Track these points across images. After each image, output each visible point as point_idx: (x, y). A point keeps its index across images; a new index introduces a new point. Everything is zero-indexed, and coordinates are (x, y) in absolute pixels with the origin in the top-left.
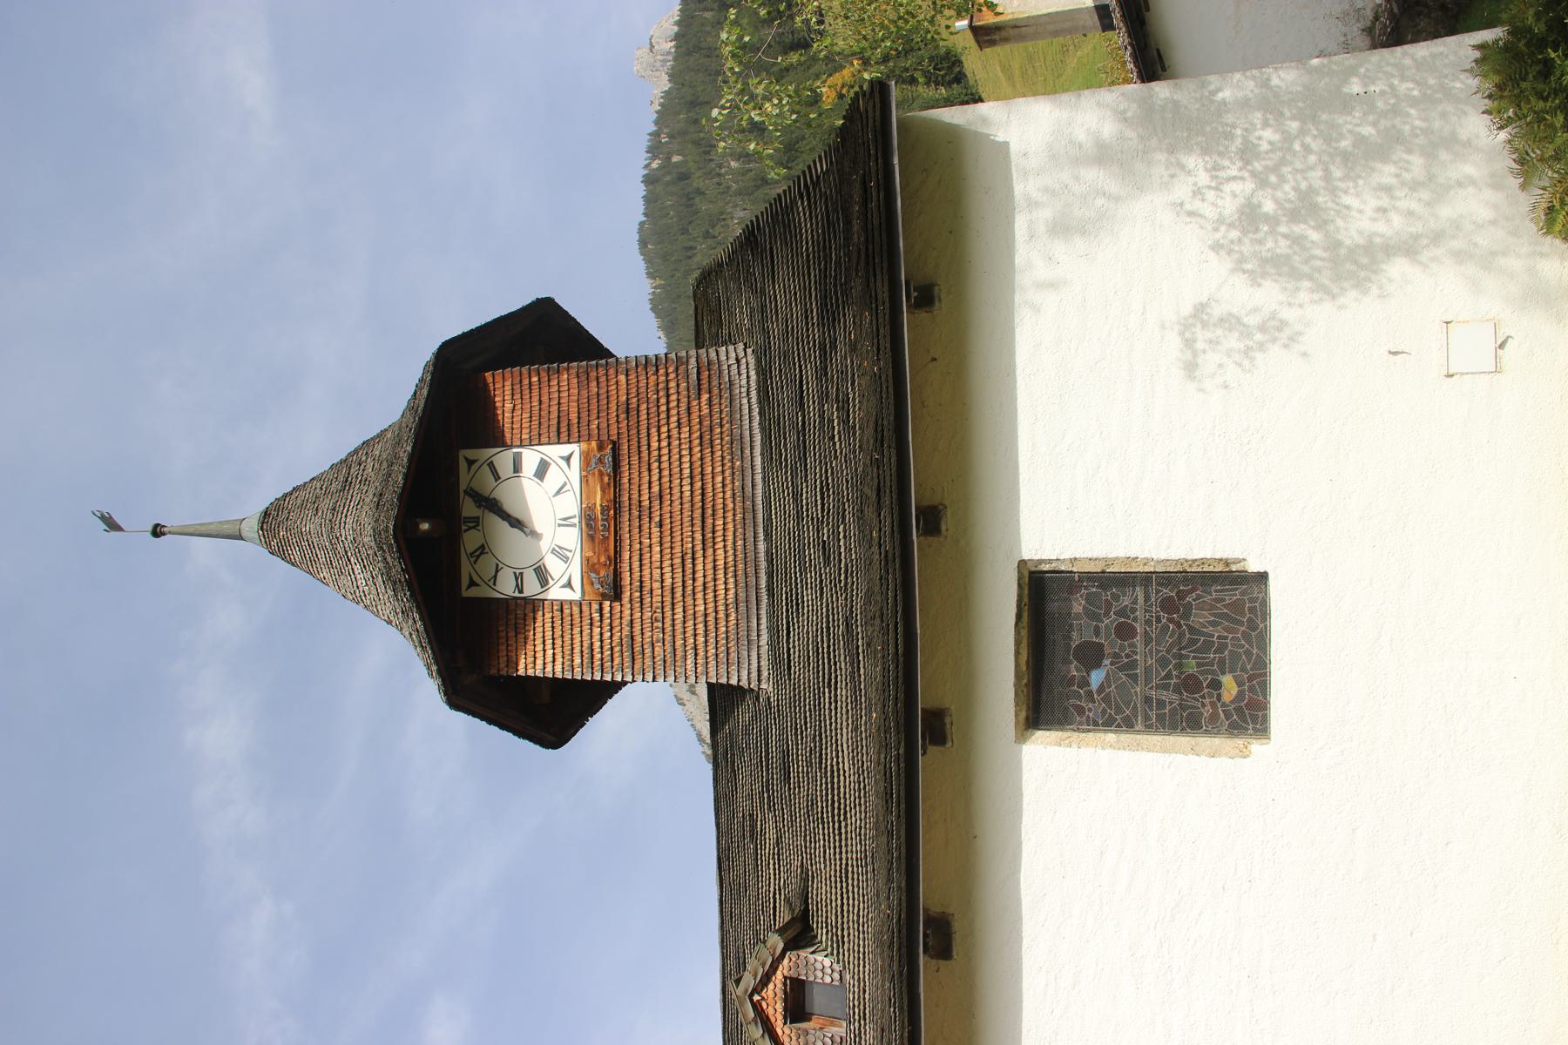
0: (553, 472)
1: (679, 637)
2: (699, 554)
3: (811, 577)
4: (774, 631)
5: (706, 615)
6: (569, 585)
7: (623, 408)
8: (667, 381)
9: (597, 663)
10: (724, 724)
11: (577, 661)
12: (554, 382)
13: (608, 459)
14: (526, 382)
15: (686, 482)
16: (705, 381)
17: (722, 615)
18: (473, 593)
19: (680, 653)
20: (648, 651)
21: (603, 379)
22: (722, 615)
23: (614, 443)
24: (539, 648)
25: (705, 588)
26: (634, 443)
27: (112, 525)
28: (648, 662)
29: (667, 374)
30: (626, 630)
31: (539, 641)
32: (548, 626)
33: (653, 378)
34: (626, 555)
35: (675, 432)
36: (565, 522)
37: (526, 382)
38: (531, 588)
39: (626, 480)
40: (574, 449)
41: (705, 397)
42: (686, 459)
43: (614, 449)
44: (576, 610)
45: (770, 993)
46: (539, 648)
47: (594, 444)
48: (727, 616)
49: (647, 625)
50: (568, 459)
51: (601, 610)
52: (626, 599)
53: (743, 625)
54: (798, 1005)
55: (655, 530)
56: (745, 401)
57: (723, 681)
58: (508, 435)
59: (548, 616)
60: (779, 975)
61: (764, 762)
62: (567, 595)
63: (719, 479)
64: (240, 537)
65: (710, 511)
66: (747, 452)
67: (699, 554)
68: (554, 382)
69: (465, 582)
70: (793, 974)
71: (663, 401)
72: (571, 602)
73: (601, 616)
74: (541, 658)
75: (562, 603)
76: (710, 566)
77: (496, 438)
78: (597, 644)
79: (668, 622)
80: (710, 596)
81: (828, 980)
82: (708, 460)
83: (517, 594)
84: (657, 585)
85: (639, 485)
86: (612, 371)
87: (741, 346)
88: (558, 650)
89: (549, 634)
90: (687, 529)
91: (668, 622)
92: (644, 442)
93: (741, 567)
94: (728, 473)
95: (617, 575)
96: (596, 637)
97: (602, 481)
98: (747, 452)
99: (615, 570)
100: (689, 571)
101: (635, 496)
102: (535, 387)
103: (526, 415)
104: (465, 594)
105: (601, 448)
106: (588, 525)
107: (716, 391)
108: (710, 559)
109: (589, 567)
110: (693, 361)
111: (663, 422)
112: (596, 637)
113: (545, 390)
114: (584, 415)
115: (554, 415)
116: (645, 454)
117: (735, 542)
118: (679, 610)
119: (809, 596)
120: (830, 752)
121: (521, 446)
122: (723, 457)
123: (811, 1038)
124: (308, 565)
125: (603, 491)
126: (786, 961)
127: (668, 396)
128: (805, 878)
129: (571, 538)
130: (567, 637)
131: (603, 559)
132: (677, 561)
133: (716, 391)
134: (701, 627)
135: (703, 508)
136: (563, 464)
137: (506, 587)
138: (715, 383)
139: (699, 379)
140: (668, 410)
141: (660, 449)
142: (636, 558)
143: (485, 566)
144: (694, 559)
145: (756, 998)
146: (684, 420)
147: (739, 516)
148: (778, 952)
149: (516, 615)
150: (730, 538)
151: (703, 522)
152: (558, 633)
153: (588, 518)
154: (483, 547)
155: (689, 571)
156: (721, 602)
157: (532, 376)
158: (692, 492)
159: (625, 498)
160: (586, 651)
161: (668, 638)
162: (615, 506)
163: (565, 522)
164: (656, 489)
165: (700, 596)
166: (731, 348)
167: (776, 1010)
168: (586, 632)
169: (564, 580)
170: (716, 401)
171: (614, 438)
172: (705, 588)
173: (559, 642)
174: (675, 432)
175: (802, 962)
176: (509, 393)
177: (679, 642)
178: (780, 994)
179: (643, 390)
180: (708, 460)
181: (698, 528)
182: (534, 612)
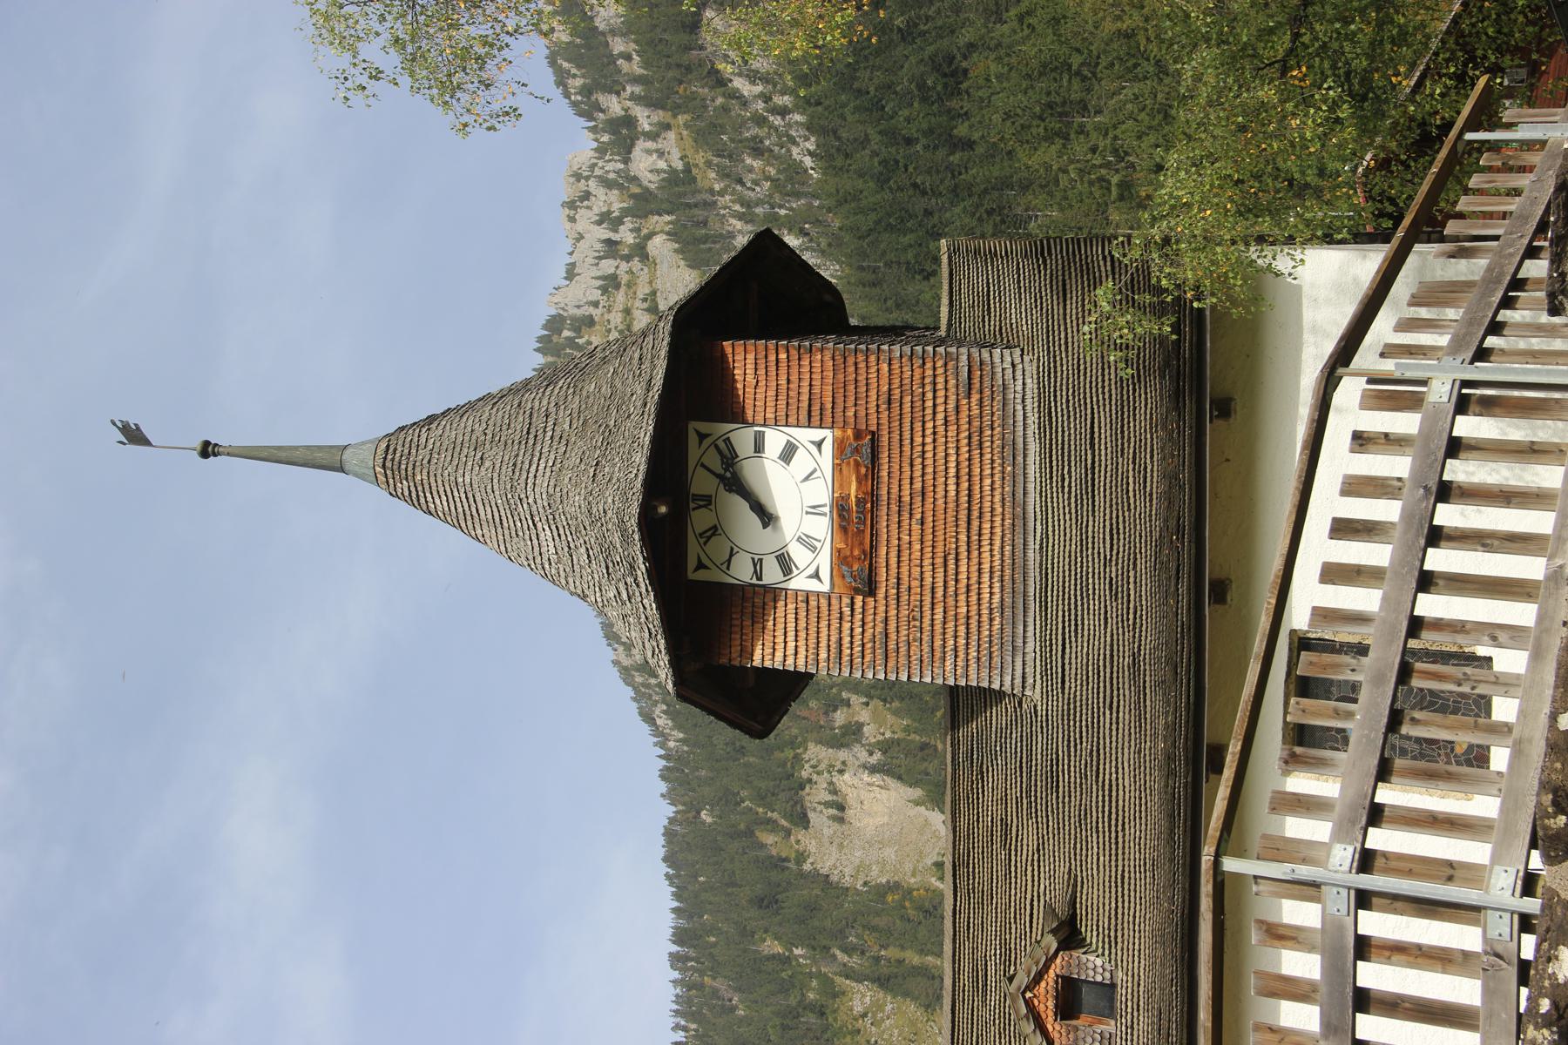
0: (800, 455)
1: (938, 637)
2: (963, 555)
3: (1094, 605)
4: (1046, 644)
5: (968, 618)
6: (816, 576)
7: (884, 398)
8: (935, 376)
9: (846, 659)
10: (969, 720)
11: (823, 655)
12: (806, 362)
13: (867, 450)
14: (772, 358)
15: (952, 481)
16: (976, 381)
17: (985, 618)
18: (701, 575)
19: (938, 654)
20: (903, 650)
21: (862, 365)
22: (985, 618)
23: (873, 433)
24: (780, 639)
25: (968, 591)
26: (896, 436)
27: (134, 436)
28: (903, 660)
29: (935, 369)
30: (880, 628)
31: (780, 632)
32: (791, 617)
33: (918, 373)
34: (883, 551)
35: (941, 430)
36: (814, 510)
37: (772, 358)
38: (772, 575)
39: (884, 473)
40: (827, 434)
41: (975, 397)
42: (953, 458)
43: (872, 440)
44: (824, 603)
45: (1042, 990)
46: (780, 639)
47: (850, 432)
48: (991, 620)
49: (903, 623)
50: (819, 444)
51: (853, 603)
52: (881, 594)
53: (1008, 630)
54: (1070, 999)
55: (916, 527)
56: (1019, 407)
57: (985, 684)
58: (749, 413)
59: (791, 606)
60: (1051, 973)
61: (1025, 766)
62: (813, 586)
63: (988, 481)
64: (341, 469)
65: (975, 514)
66: (1020, 459)
67: (963, 555)
68: (806, 362)
69: (692, 563)
70: (1065, 972)
71: (929, 395)
72: (818, 594)
73: (852, 610)
74: (776, 648)
75: (808, 594)
76: (974, 568)
77: (736, 414)
78: (847, 640)
79: (927, 621)
80: (974, 598)
81: (1099, 979)
82: (976, 460)
83: (754, 581)
84: (915, 583)
85: (894, 478)
86: (873, 358)
87: (1017, 352)
88: (802, 643)
89: (791, 627)
90: (951, 530)
91: (927, 621)
92: (907, 435)
93: (1008, 572)
94: (997, 477)
95: (872, 570)
96: (846, 632)
97: (858, 472)
98: (1020, 459)
99: (871, 564)
100: (951, 571)
101: (895, 490)
102: (783, 365)
103: (772, 393)
104: (692, 576)
105: (858, 435)
106: (840, 516)
107: (987, 392)
108: (975, 561)
109: (841, 559)
110: (964, 358)
111: (928, 418)
112: (846, 632)
113: (794, 371)
114: (840, 401)
115: (805, 397)
116: (907, 449)
117: (1002, 547)
118: (939, 610)
119: (1091, 622)
120: (1108, 769)
121: (764, 425)
122: (993, 461)
123: (1081, 1034)
124: (461, 520)
125: (859, 482)
126: (1058, 960)
127: (935, 391)
128: (1074, 886)
129: (821, 528)
130: (813, 630)
131: (856, 553)
132: (939, 561)
133: (987, 392)
134: (962, 629)
135: (969, 509)
136: (814, 449)
137: (742, 572)
138: (987, 383)
139: (970, 378)
140: (935, 406)
141: (923, 445)
142: (893, 554)
143: (717, 549)
144: (957, 560)
145: (1028, 995)
146: (952, 418)
147: (1008, 522)
148: (1052, 951)
149: (756, 601)
150: (998, 543)
151: (969, 523)
152: (802, 624)
153: (841, 508)
154: (715, 528)
155: (951, 571)
156: (985, 606)
157: (780, 351)
158: (958, 492)
159: (884, 491)
160: (833, 646)
161: (926, 638)
162: (871, 499)
163: (814, 510)
164: (918, 485)
165: (962, 598)
166: (1007, 352)
167: (1047, 1007)
168: (835, 624)
169: (811, 571)
170: (987, 402)
171: (874, 428)
172: (968, 591)
173: (802, 635)
174: (941, 430)
175: (1074, 962)
176: (747, 363)
177: (938, 643)
178: (1052, 992)
179: (907, 381)
180: (976, 460)
181: (962, 529)
182: (775, 601)
